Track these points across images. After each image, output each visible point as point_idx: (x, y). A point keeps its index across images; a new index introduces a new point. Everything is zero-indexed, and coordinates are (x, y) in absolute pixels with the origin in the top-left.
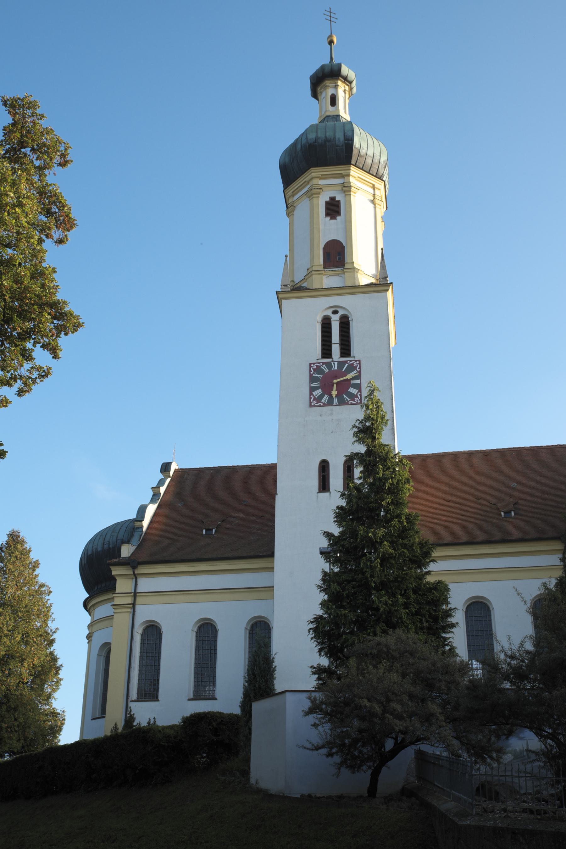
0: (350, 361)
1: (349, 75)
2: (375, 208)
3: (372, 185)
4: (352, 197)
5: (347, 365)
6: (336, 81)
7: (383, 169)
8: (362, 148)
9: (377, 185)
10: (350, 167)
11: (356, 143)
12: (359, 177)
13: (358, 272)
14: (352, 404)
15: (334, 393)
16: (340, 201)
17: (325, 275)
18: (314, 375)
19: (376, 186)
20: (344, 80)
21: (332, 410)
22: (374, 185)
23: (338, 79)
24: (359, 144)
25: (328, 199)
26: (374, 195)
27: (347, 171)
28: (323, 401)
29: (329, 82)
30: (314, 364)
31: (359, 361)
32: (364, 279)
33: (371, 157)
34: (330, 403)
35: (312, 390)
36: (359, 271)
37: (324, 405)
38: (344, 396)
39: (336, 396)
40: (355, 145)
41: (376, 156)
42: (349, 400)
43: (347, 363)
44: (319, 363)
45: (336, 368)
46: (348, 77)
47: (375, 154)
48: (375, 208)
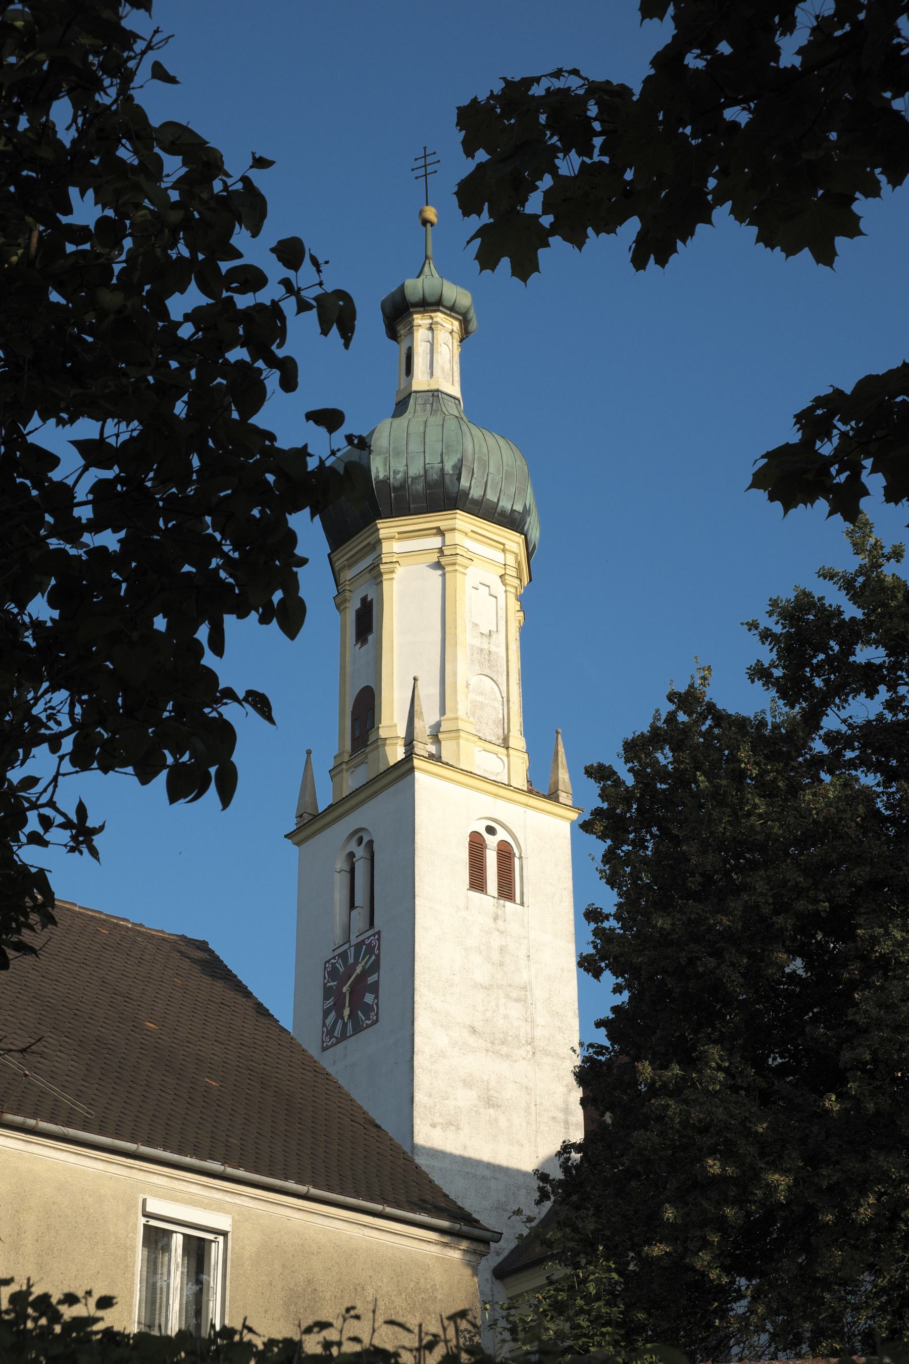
0: (368, 938)
1: (426, 292)
2: (444, 575)
3: (435, 531)
4: (385, 583)
5: (364, 947)
6: (410, 319)
7: (457, 482)
8: (394, 472)
9: (443, 525)
10: (376, 524)
11: (378, 472)
12: (399, 533)
13: (384, 745)
14: (368, 1026)
15: (346, 1012)
16: (372, 599)
17: (347, 770)
18: (328, 984)
19: (442, 528)
20: (422, 309)
21: (346, 1048)
22: (438, 528)
23: (411, 314)
24: (385, 471)
25: (358, 605)
26: (441, 550)
27: (375, 535)
28: (336, 1034)
29: (401, 326)
30: (328, 961)
31: (379, 933)
32: (397, 753)
33: (420, 477)
34: (344, 1037)
35: (326, 1013)
36: (388, 742)
37: (339, 1041)
38: (360, 1013)
39: (349, 1016)
40: (377, 477)
41: (432, 468)
42: (364, 1019)
43: (365, 944)
44: (334, 958)
45: (352, 961)
46: (427, 295)
47: (427, 466)
48: (444, 575)
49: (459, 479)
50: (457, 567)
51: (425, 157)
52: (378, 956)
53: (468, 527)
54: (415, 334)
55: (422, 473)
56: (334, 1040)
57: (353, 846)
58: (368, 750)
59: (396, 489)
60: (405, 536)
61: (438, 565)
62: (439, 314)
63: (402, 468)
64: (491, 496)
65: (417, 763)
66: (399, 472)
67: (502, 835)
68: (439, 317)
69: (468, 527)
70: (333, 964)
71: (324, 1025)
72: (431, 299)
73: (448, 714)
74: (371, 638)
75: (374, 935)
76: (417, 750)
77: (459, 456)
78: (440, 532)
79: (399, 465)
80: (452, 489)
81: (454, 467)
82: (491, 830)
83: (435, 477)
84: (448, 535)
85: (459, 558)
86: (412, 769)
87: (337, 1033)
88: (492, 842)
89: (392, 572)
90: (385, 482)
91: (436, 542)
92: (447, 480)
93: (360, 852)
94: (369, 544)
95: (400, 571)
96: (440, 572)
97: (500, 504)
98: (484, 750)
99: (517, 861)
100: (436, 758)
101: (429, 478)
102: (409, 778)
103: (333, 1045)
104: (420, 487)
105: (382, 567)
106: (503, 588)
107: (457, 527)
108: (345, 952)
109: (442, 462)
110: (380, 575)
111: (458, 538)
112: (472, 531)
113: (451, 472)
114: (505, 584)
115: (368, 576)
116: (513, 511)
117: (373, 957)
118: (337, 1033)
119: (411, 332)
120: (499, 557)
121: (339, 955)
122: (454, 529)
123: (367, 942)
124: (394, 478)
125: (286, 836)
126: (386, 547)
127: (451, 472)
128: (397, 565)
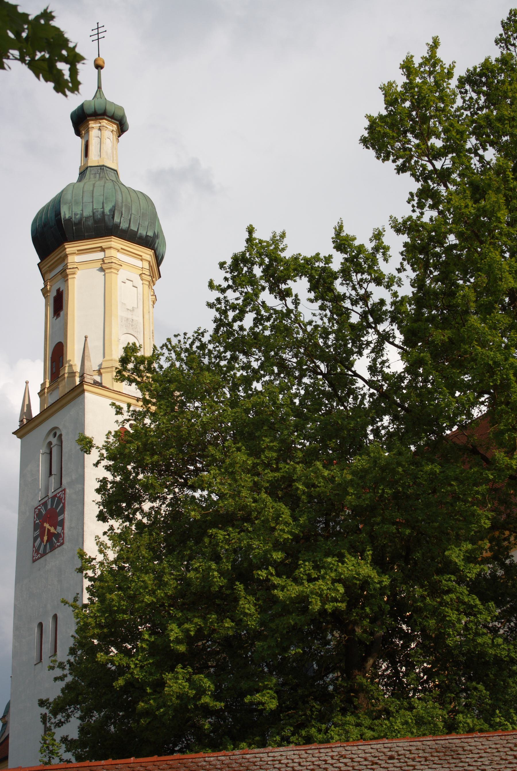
1: (96, 107)
2: (105, 275)
8: (75, 214)
9: (104, 245)
11: (65, 214)
12: (78, 251)
15: (46, 538)
21: (46, 560)
22: (101, 247)
23: (88, 121)
26: (103, 261)
30: (36, 508)
31: (64, 490)
33: (90, 217)
34: (45, 554)
35: (35, 539)
37: (43, 555)
40: (65, 217)
41: (97, 211)
44: (40, 506)
48: (105, 275)
49: (113, 218)
50: (112, 270)
51: (98, 28)
52: (64, 504)
53: (119, 246)
54: (90, 132)
55: (91, 214)
56: (39, 555)
57: (51, 438)
58: (59, 380)
59: (76, 224)
61: (102, 270)
62: (104, 121)
63: (79, 212)
64: (134, 228)
65: (86, 387)
66: (77, 214)
68: (104, 122)
69: (119, 246)
70: (39, 509)
71: (34, 546)
72: (99, 112)
73: (107, 358)
74: (62, 313)
75: (62, 491)
76: (86, 380)
77: (113, 204)
78: (103, 250)
79: (77, 210)
80: (110, 224)
81: (110, 210)
83: (99, 216)
84: (107, 251)
85: (113, 265)
86: (83, 391)
87: (41, 551)
89: (74, 274)
90: (70, 219)
91: (100, 255)
92: (106, 218)
93: (55, 441)
94: (61, 257)
95: (79, 273)
96: (103, 273)
97: (139, 232)
100: (97, 384)
101: (96, 218)
102: (81, 397)
103: (39, 558)
104: (90, 222)
105: (68, 271)
106: (141, 282)
107: (112, 246)
108: (46, 502)
109: (103, 208)
110: (67, 275)
111: (112, 253)
112: (122, 249)
113: (108, 214)
114: (142, 280)
115: (60, 277)
116: (147, 236)
117: (61, 505)
118: (41, 551)
119: (87, 132)
120: (139, 263)
121: (43, 504)
122: (110, 248)
123: (58, 495)
124: (75, 218)
125: (13, 433)
126: (70, 259)
127: (108, 214)
128: (76, 270)
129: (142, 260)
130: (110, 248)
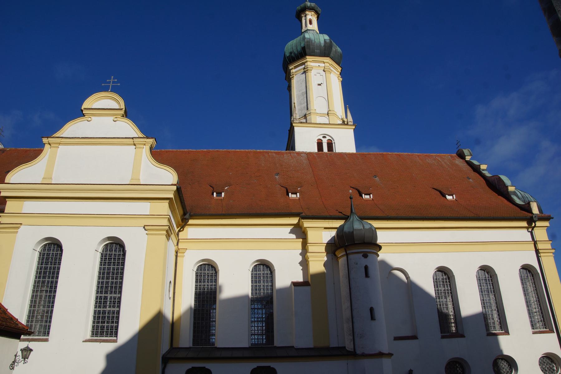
22: (303, 62)
60: (296, 67)
67: (328, 138)
73: (309, 109)
78: (304, 64)
82: (324, 137)
88: (325, 142)
89: (293, 77)
98: (321, 116)
99: (334, 144)
107: (308, 60)
111: (308, 63)
112: (312, 61)
129: (324, 63)
130: (307, 62)
